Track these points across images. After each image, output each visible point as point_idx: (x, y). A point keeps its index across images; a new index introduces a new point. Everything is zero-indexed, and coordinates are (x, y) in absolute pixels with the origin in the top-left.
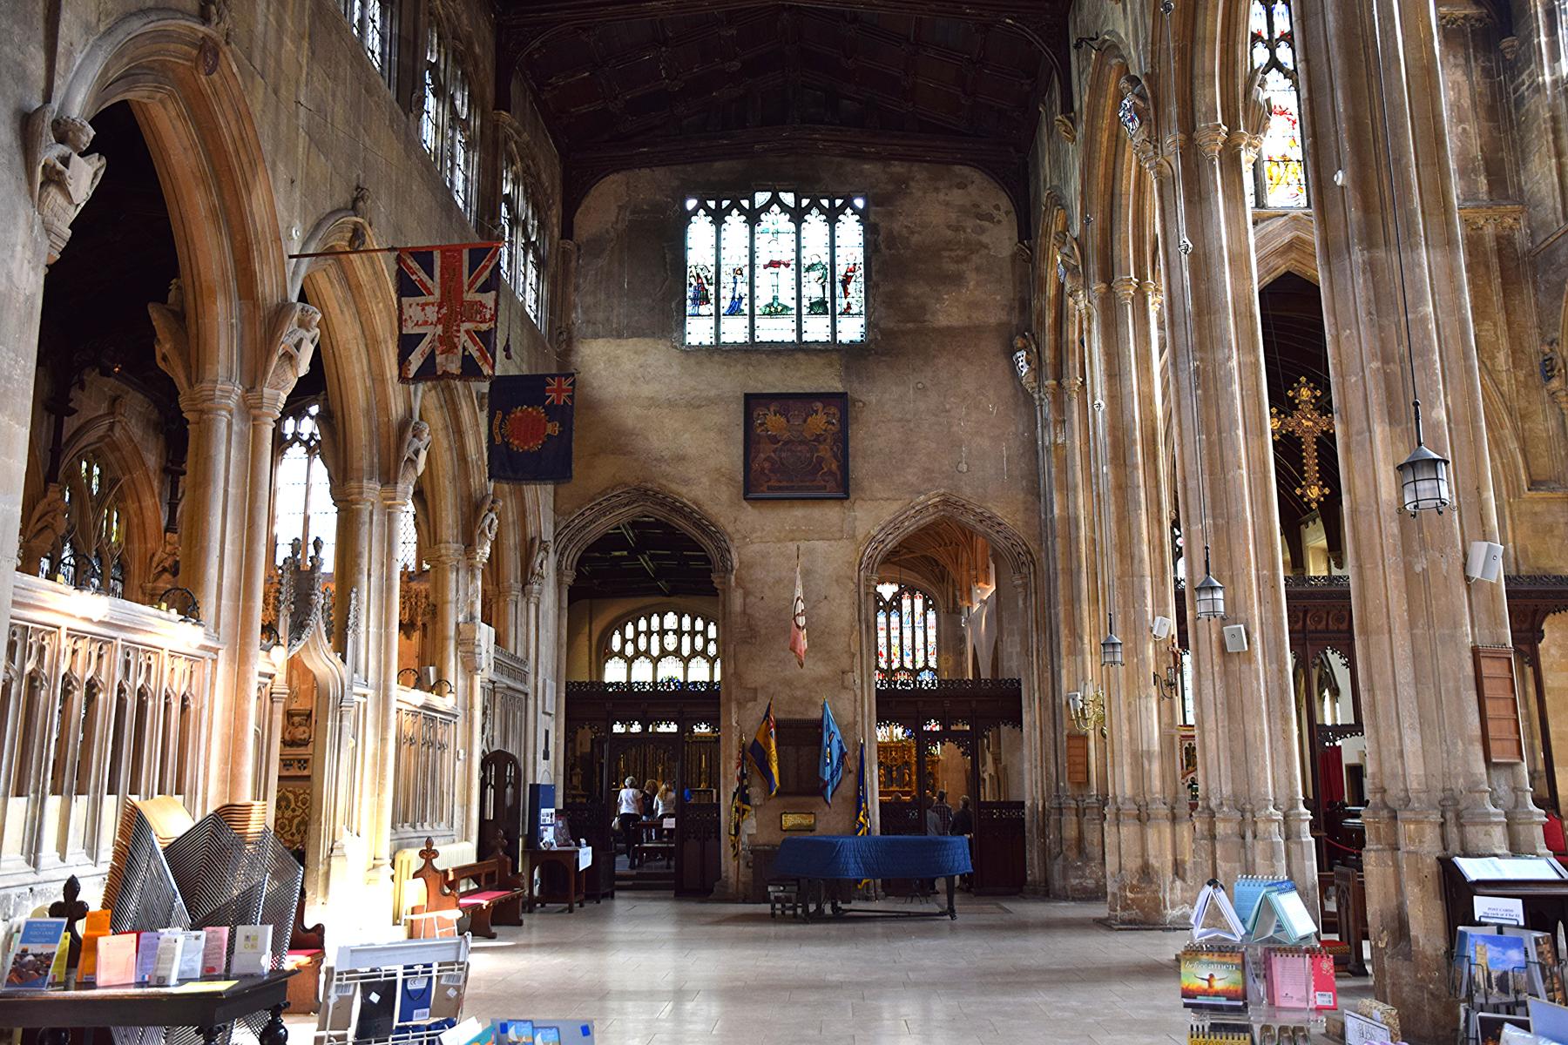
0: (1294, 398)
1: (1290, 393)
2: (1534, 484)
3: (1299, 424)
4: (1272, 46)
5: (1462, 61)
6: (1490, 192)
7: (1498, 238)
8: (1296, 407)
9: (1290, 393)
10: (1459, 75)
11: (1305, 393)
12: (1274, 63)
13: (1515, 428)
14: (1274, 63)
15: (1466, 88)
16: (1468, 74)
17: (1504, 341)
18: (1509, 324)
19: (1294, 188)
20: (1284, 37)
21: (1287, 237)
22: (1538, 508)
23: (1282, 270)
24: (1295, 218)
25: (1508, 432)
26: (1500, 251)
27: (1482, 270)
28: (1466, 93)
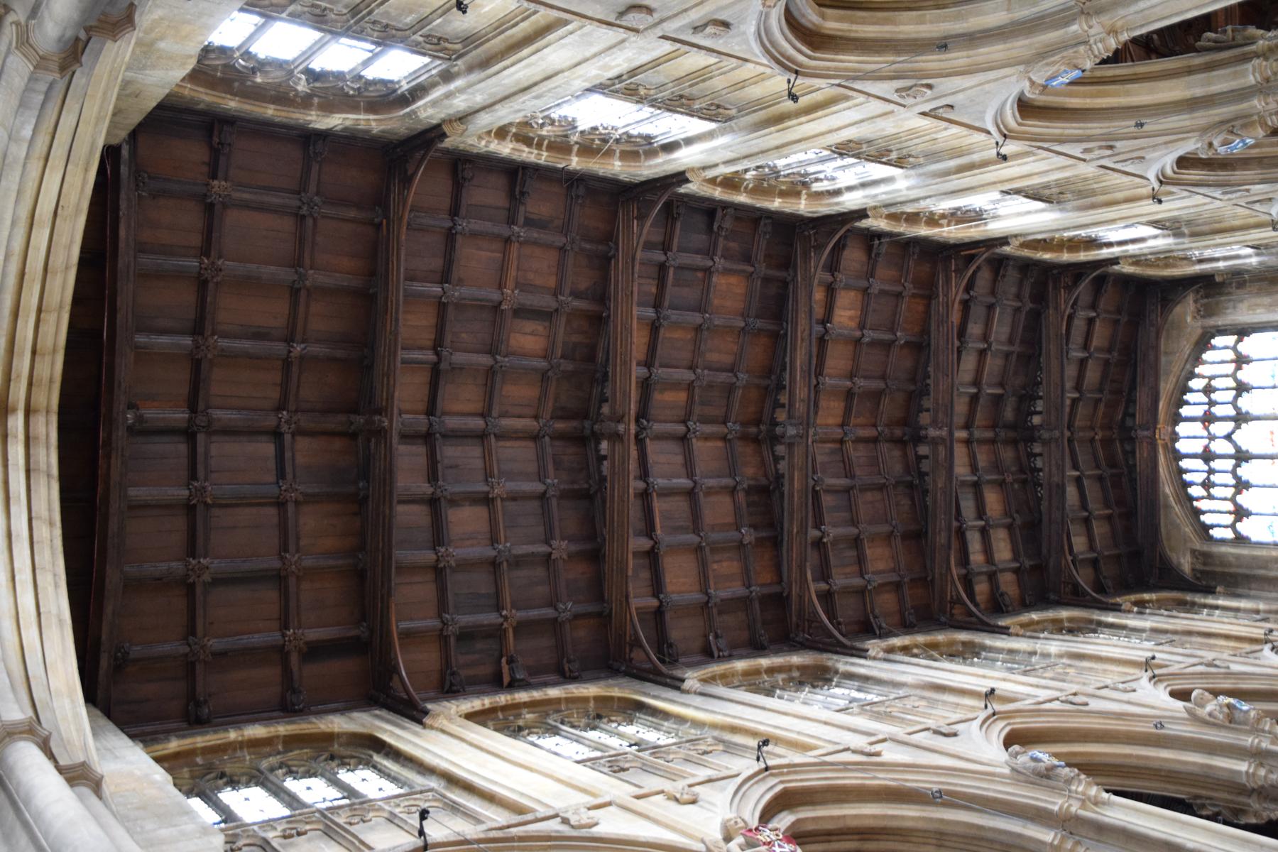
4: (1212, 438)
5: (1231, 304)
10: (1243, 306)
12: (1228, 437)
14: (1228, 437)
16: (1242, 301)
20: (1207, 428)
28: (1258, 300)
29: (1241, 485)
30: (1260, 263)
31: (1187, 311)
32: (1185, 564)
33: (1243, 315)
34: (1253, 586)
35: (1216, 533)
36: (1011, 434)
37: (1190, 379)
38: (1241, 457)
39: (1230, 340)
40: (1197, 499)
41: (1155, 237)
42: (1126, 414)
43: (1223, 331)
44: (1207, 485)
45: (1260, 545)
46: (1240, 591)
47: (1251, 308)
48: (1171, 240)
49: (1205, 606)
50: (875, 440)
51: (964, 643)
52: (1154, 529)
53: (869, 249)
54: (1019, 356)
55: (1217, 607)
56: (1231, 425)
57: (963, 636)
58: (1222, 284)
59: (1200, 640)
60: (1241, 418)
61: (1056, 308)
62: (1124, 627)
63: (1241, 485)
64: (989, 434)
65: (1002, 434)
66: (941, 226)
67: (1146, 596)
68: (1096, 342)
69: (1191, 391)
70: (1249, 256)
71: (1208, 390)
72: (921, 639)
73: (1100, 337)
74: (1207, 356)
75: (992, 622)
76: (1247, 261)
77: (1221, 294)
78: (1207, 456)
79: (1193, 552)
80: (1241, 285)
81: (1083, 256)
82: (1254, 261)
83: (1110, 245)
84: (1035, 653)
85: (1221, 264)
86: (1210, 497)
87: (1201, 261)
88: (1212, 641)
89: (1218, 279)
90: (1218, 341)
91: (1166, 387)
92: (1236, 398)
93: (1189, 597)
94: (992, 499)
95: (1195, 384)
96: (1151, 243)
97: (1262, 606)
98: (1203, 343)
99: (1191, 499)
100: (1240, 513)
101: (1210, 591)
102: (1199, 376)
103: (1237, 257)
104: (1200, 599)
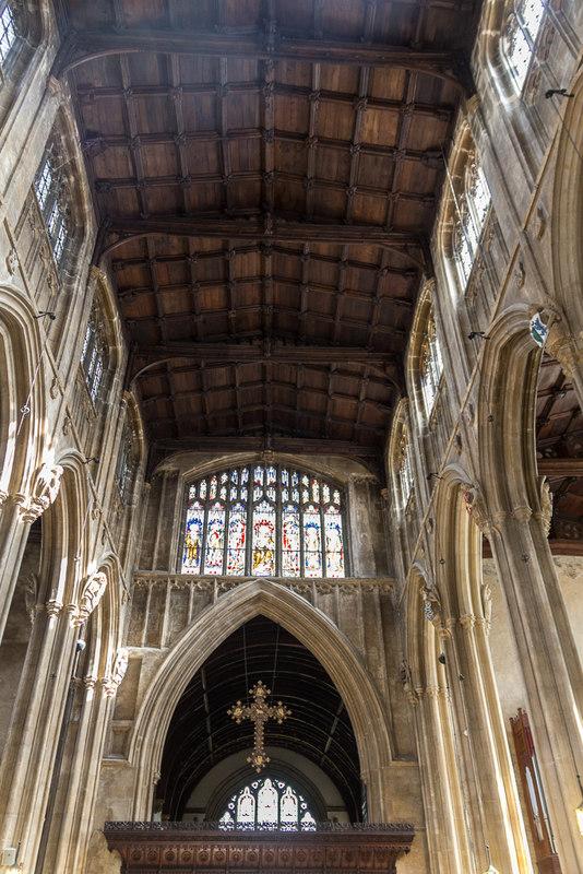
0: (253, 694)
1: (251, 692)
2: (397, 756)
3: (255, 712)
4: (264, 488)
6: (377, 571)
7: (381, 597)
8: (252, 701)
9: (251, 692)
10: (363, 507)
11: (260, 692)
12: (265, 498)
13: (386, 718)
14: (265, 498)
15: (366, 513)
17: (383, 660)
18: (386, 648)
19: (268, 566)
21: (255, 593)
22: (400, 773)
23: (253, 614)
24: (261, 582)
25: (381, 719)
26: (381, 605)
27: (371, 615)
28: (366, 516)
29: (228, 506)
30: (395, 514)
31: (360, 473)
32: (168, 467)
33: (357, 509)
34: (151, 508)
35: (193, 490)
36: (268, 320)
37: (309, 477)
38: (249, 506)
39: (337, 501)
40: (219, 480)
41: (424, 416)
42: (282, 432)
43: (343, 497)
44: (229, 485)
45: (184, 515)
46: (147, 501)
47: (361, 513)
48: (421, 426)
49: (135, 473)
50: (262, 170)
51: (83, 229)
52: (195, 447)
53: (433, 149)
54: (332, 327)
55: (134, 480)
56: (274, 500)
57: (89, 228)
58: (379, 495)
59: (97, 435)
60: (278, 507)
61: (367, 357)
62: (109, 388)
63: (228, 506)
64: (269, 299)
65: (269, 311)
66: (448, 220)
67: (141, 431)
68: (339, 401)
69: (300, 477)
70: (401, 505)
71: (300, 487)
72: (85, 188)
73: (344, 406)
74: (326, 491)
75: (103, 258)
76: (397, 505)
77: (371, 495)
78: (250, 485)
79: (178, 472)
80: (378, 507)
81: (410, 370)
82: (398, 509)
83: (419, 388)
84: (72, 273)
85: (395, 489)
86: (218, 489)
87: (398, 477)
88: (95, 442)
89: (383, 491)
90: (337, 495)
91: (303, 459)
92: (294, 504)
93: (142, 463)
94: (211, 298)
95: (305, 480)
96: (419, 414)
97: (134, 506)
98: (335, 485)
99: (218, 475)
100: (207, 505)
101: (147, 479)
102: (310, 485)
103: (400, 499)
104: (142, 468)
